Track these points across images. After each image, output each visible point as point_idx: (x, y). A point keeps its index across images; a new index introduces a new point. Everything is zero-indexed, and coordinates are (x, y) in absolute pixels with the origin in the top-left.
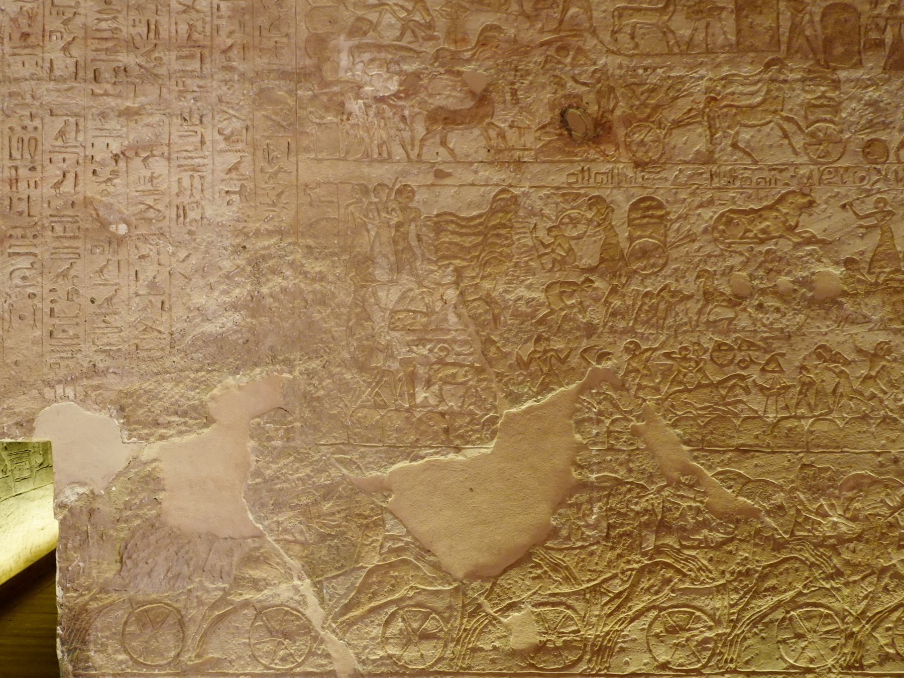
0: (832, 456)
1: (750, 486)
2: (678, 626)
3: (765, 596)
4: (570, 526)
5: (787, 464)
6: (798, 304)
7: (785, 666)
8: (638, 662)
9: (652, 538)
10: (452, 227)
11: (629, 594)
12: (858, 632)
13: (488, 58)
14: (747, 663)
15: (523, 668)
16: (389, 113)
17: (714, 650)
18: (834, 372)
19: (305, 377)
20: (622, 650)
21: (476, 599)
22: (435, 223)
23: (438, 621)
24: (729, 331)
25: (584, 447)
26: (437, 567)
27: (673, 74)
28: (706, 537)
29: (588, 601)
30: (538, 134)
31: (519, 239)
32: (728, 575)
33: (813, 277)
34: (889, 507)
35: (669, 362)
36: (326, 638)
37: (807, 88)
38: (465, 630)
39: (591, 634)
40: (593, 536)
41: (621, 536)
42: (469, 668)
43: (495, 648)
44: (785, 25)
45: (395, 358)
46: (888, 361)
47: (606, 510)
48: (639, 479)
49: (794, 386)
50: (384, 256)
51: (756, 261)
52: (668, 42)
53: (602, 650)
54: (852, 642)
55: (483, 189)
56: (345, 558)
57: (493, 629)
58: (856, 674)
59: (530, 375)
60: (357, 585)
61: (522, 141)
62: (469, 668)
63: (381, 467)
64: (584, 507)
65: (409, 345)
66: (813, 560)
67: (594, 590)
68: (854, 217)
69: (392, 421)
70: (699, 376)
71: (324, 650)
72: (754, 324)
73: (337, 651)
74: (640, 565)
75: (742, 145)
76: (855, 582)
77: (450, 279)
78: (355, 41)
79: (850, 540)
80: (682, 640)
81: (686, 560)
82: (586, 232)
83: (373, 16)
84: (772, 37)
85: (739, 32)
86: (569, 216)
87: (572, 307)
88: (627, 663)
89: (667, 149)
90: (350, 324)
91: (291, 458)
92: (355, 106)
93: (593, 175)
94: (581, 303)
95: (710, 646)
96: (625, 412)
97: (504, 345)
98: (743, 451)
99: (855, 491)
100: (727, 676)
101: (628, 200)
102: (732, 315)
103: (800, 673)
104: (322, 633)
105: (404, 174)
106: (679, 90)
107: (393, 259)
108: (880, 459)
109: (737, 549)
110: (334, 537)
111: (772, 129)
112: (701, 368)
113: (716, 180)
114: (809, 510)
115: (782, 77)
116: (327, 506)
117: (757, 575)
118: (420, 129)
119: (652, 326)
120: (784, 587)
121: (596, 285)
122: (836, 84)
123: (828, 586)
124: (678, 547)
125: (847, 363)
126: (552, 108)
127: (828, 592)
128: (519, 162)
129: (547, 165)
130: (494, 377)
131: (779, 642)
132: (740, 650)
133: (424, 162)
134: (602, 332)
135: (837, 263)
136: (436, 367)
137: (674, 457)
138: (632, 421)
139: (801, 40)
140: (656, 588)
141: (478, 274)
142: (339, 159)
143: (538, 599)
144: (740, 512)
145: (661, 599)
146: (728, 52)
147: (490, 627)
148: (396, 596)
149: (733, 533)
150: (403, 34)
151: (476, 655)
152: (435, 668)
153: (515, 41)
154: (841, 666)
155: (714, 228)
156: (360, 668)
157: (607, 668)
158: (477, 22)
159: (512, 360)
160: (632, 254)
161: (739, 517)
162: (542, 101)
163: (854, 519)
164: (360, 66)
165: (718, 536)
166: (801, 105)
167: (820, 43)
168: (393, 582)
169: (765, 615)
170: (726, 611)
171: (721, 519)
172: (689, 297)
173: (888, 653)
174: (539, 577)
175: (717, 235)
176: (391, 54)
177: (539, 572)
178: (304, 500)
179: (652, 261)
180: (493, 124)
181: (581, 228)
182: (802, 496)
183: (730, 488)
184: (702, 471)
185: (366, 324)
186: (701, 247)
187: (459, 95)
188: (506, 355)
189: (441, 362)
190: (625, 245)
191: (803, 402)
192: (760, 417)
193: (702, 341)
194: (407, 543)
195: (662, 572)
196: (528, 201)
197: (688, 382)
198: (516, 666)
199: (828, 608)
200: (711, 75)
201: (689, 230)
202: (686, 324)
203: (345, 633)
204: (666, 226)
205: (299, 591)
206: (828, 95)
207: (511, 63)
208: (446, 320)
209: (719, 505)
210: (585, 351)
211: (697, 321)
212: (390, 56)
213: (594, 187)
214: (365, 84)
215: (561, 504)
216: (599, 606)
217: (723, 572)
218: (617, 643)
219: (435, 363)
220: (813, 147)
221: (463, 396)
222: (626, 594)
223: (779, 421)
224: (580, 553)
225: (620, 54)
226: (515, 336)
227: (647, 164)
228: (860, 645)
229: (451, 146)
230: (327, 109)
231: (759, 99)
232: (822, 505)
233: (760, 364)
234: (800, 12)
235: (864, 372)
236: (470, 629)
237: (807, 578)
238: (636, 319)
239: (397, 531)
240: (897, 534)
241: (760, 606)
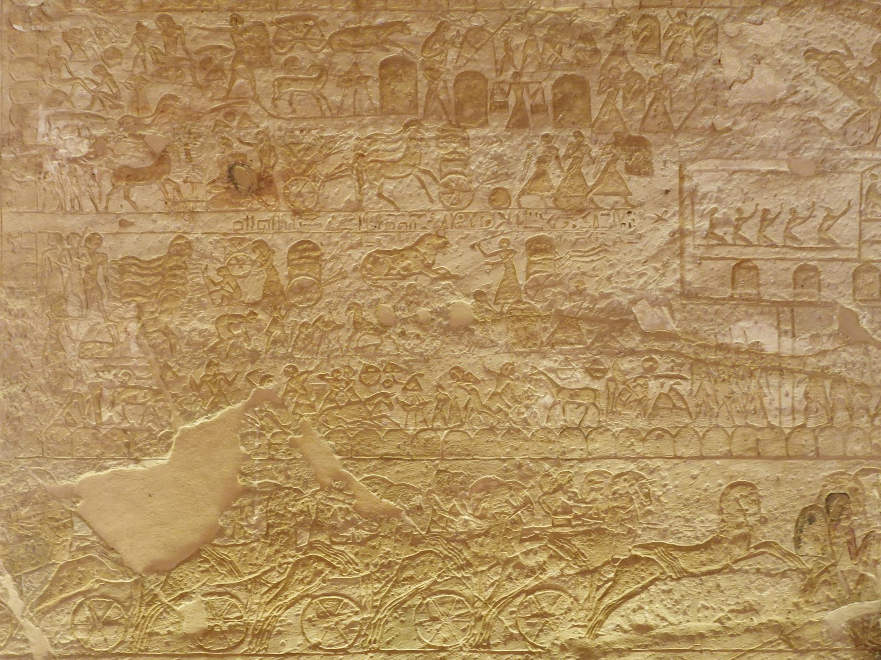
0: (464, 463)
1: (392, 489)
2: (328, 611)
3: (404, 585)
4: (234, 527)
6: (435, 331)
7: (422, 645)
8: (292, 644)
9: (307, 536)
10: (134, 269)
11: (286, 584)
12: (487, 615)
13: (167, 123)
14: (388, 643)
15: (192, 649)
16: (80, 171)
17: (360, 632)
18: (466, 390)
20: (280, 633)
21: (152, 590)
22: (120, 266)
23: (120, 610)
24: (376, 355)
25: (247, 457)
27: (325, 134)
28: (353, 535)
29: (250, 591)
30: (208, 188)
31: (192, 279)
32: (372, 567)
33: (449, 308)
34: (513, 507)
35: (323, 383)
37: (441, 145)
38: (143, 617)
39: (252, 619)
40: (254, 534)
41: (279, 534)
42: (147, 650)
43: (170, 633)
44: (423, 91)
45: (85, 383)
46: (512, 380)
47: (266, 512)
48: (296, 485)
49: (431, 402)
50: (76, 295)
51: (398, 294)
52: (321, 108)
53: (261, 633)
54: (481, 624)
55: (161, 236)
56: (39, 557)
58: (483, 652)
59: (201, 396)
61: (195, 194)
62: (147, 650)
63: (70, 477)
64: (246, 509)
65: (96, 371)
66: (446, 553)
67: (254, 581)
68: (482, 255)
70: (350, 395)
71: (23, 636)
72: (398, 349)
74: (295, 559)
75: (386, 195)
76: (482, 572)
77: (133, 313)
78: (52, 111)
79: (479, 536)
81: (335, 554)
82: (250, 271)
83: (67, 89)
84: (411, 102)
85: (382, 97)
86: (236, 258)
87: (238, 336)
88: (283, 644)
89: (320, 198)
90: (46, 354)
92: (51, 166)
93: (256, 222)
94: (246, 333)
96: (285, 426)
97: (179, 371)
98: (387, 459)
99: (483, 493)
100: (370, 654)
101: (287, 243)
102: (378, 342)
103: (435, 652)
104: (22, 621)
105: (92, 223)
106: (330, 149)
107: (83, 297)
108: (505, 465)
110: (30, 537)
111: (411, 181)
112: (351, 388)
113: (364, 225)
115: (419, 136)
116: (24, 511)
117: (397, 567)
118: (107, 186)
119: (308, 352)
121: (260, 317)
122: (466, 141)
123: (459, 576)
124: (328, 542)
125: (477, 382)
126: (220, 164)
127: (459, 581)
128: (192, 212)
129: (216, 215)
131: (416, 624)
132: (383, 632)
133: (111, 214)
134: (264, 358)
135: (467, 296)
136: (119, 390)
138: (290, 434)
139: (436, 104)
141: (157, 309)
142: (37, 212)
143: (206, 589)
144: (384, 512)
145: (314, 588)
146: (373, 115)
147: (165, 614)
148: (84, 588)
150: (92, 103)
151: (153, 638)
152: (116, 651)
153: (190, 108)
154: (471, 645)
155: (363, 266)
158: (156, 93)
159: (186, 384)
160: (291, 290)
162: (212, 160)
163: (482, 517)
164: (55, 132)
165: (364, 533)
166: (436, 160)
167: (453, 106)
168: (81, 576)
169: (405, 601)
172: (340, 327)
173: (512, 634)
174: (207, 571)
175: (364, 272)
176: (82, 122)
177: (207, 566)
179: (308, 296)
180: (169, 179)
181: (247, 268)
182: (437, 498)
183: (375, 491)
185: (59, 353)
186: (351, 283)
187: (140, 155)
188: (180, 379)
189: (124, 385)
190: (284, 282)
191: (439, 416)
192: (401, 430)
193: (352, 365)
194: (93, 542)
196: (201, 246)
198: (186, 648)
199: (460, 595)
200: (358, 135)
201: (341, 269)
202: (337, 350)
203: (40, 620)
204: (321, 266)
206: (459, 150)
207: (185, 127)
208: (129, 349)
209: (365, 507)
210: (249, 374)
211: (347, 347)
212: (81, 123)
213: (258, 233)
214: (60, 147)
215: (228, 507)
216: (259, 595)
217: (367, 565)
219: (120, 386)
220: (446, 196)
221: (143, 415)
222: (283, 584)
223: (418, 433)
224: (242, 549)
225: (281, 118)
226: (189, 362)
227: (304, 212)
228: (487, 626)
229: (133, 199)
230: (26, 168)
231: (400, 155)
232: (454, 506)
233: (402, 384)
234: (436, 79)
235: (491, 389)
237: (441, 569)
238: (294, 346)
240: (519, 529)
241: (400, 594)
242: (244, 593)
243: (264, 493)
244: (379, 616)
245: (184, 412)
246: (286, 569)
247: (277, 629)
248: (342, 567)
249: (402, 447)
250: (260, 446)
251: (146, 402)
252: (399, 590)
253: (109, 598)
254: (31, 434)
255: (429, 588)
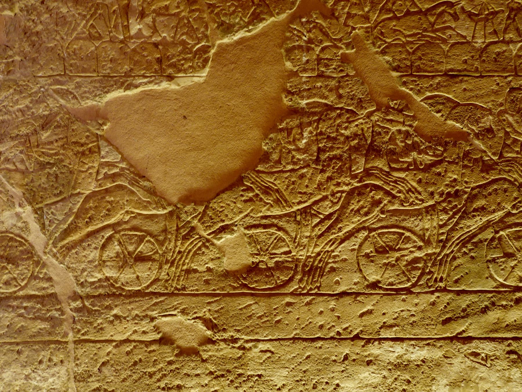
1: (458, 110)
2: (387, 246)
3: (474, 216)
4: (281, 151)
5: (495, 87)
7: (495, 285)
9: (362, 161)
11: (339, 216)
14: (456, 281)
15: (235, 288)
17: (423, 269)
19: (25, 13)
20: (333, 270)
21: (189, 222)
25: (295, 74)
26: (152, 192)
28: (415, 160)
29: (299, 223)
32: (437, 197)
36: (48, 262)
38: (180, 252)
39: (302, 254)
40: (303, 159)
41: (330, 159)
42: (184, 289)
43: (209, 270)
47: (316, 135)
48: (348, 105)
49: (503, 11)
56: (63, 185)
57: (206, 251)
59: (241, 6)
60: (75, 210)
62: (184, 289)
63: (96, 96)
64: (294, 132)
67: (304, 212)
69: (106, 52)
71: (46, 274)
73: (58, 275)
80: (392, 260)
81: (395, 182)
88: (337, 283)
91: (11, 91)
95: (420, 265)
96: (335, 39)
98: (451, 76)
100: (437, 294)
103: (510, 292)
104: (44, 258)
109: (446, 171)
110: (53, 165)
114: (518, 132)
116: (45, 135)
120: (493, 207)
124: (387, 170)
130: (206, 8)
131: (488, 261)
132: (450, 270)
137: (384, 83)
138: (341, 48)
140: (366, 209)
143: (249, 221)
145: (371, 220)
147: (203, 249)
148: (112, 221)
149: (442, 154)
151: (190, 276)
152: (150, 290)
156: (79, 290)
157: (318, 288)
161: (448, 140)
165: (428, 159)
168: (109, 206)
169: (474, 235)
170: (435, 232)
171: (430, 142)
174: (250, 200)
177: (251, 195)
178: (24, 130)
182: (510, 119)
183: (439, 112)
184: (411, 96)
191: (511, 27)
192: (468, 42)
194: (122, 169)
195: (371, 194)
197: (397, 10)
203: (65, 256)
205: (21, 218)
215: (274, 129)
216: (310, 227)
217: (432, 194)
218: (327, 263)
222: (336, 215)
223: (487, 46)
224: (291, 176)
236: (184, 251)
237: (516, 199)
239: (112, 158)
241: (469, 227)
242: (293, 225)
243: (314, 114)
244: (446, 251)
245: (222, 23)
246: (340, 199)
247: (330, 265)
248: (402, 196)
249: (469, 62)
250: (308, 61)
251: (179, 13)
252: (468, 222)
253: (141, 231)
254: (52, 48)
255: (501, 220)
